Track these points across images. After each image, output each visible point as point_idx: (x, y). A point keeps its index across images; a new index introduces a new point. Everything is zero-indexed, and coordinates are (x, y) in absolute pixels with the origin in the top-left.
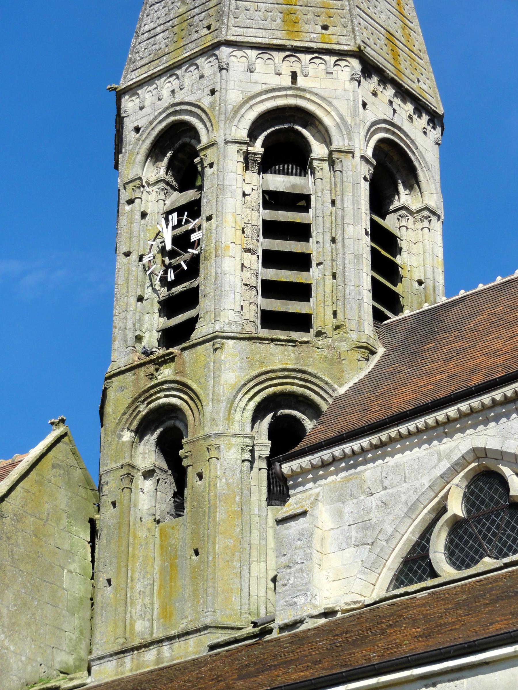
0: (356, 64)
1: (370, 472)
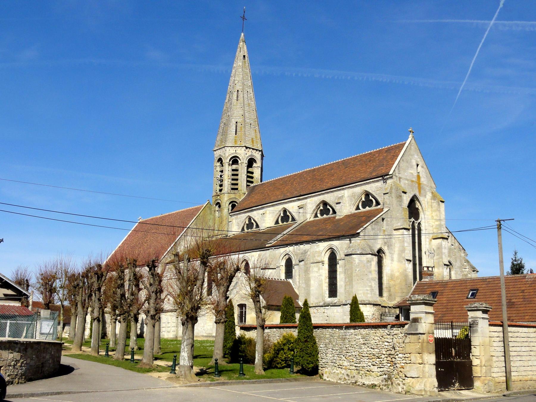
0: (245, 148)
1: (239, 216)
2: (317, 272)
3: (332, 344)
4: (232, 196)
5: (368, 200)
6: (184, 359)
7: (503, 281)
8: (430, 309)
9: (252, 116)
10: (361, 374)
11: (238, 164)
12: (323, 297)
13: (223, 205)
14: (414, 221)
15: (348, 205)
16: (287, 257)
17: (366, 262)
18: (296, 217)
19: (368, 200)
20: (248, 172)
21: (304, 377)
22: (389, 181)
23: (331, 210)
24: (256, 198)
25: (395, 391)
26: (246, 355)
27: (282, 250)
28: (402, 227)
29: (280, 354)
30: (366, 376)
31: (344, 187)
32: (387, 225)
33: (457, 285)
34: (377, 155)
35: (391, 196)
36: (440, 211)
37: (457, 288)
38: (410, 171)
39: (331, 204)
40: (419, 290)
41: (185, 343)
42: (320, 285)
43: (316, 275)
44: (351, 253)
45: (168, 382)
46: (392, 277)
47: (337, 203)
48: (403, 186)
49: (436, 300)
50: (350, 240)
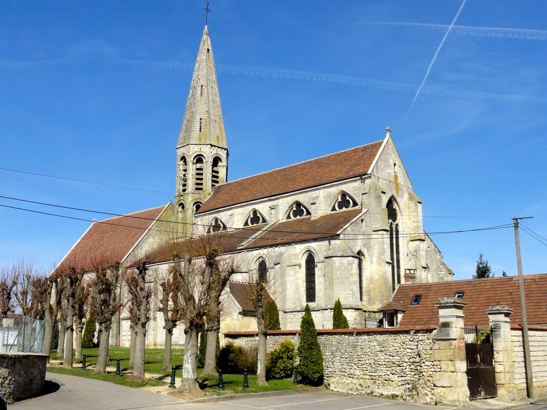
1: (204, 217)
2: (294, 276)
3: (340, 351)
4: (197, 196)
5: (345, 200)
6: (188, 372)
7: (521, 283)
8: (460, 313)
9: (217, 112)
10: (377, 384)
11: (202, 163)
12: (300, 301)
13: (187, 206)
14: (391, 223)
15: (323, 205)
16: (261, 260)
17: (347, 264)
18: (267, 218)
19: (345, 200)
20: (213, 171)
21: (308, 388)
22: (368, 181)
23: (305, 210)
24: (223, 197)
25: (422, 401)
26: (235, 364)
27: (255, 253)
28: (381, 228)
29: (278, 363)
30: (384, 385)
31: (319, 187)
32: (366, 227)
33: (441, 288)
34: (352, 154)
35: (369, 196)
36: (417, 212)
37: (441, 291)
38: (388, 171)
39: (305, 204)
40: (402, 294)
41: (189, 353)
42: (297, 289)
43: (293, 278)
44: (331, 255)
45: (171, 398)
46: (371, 281)
47: (312, 204)
48: (381, 185)
49: (466, 302)
50: (329, 242)
